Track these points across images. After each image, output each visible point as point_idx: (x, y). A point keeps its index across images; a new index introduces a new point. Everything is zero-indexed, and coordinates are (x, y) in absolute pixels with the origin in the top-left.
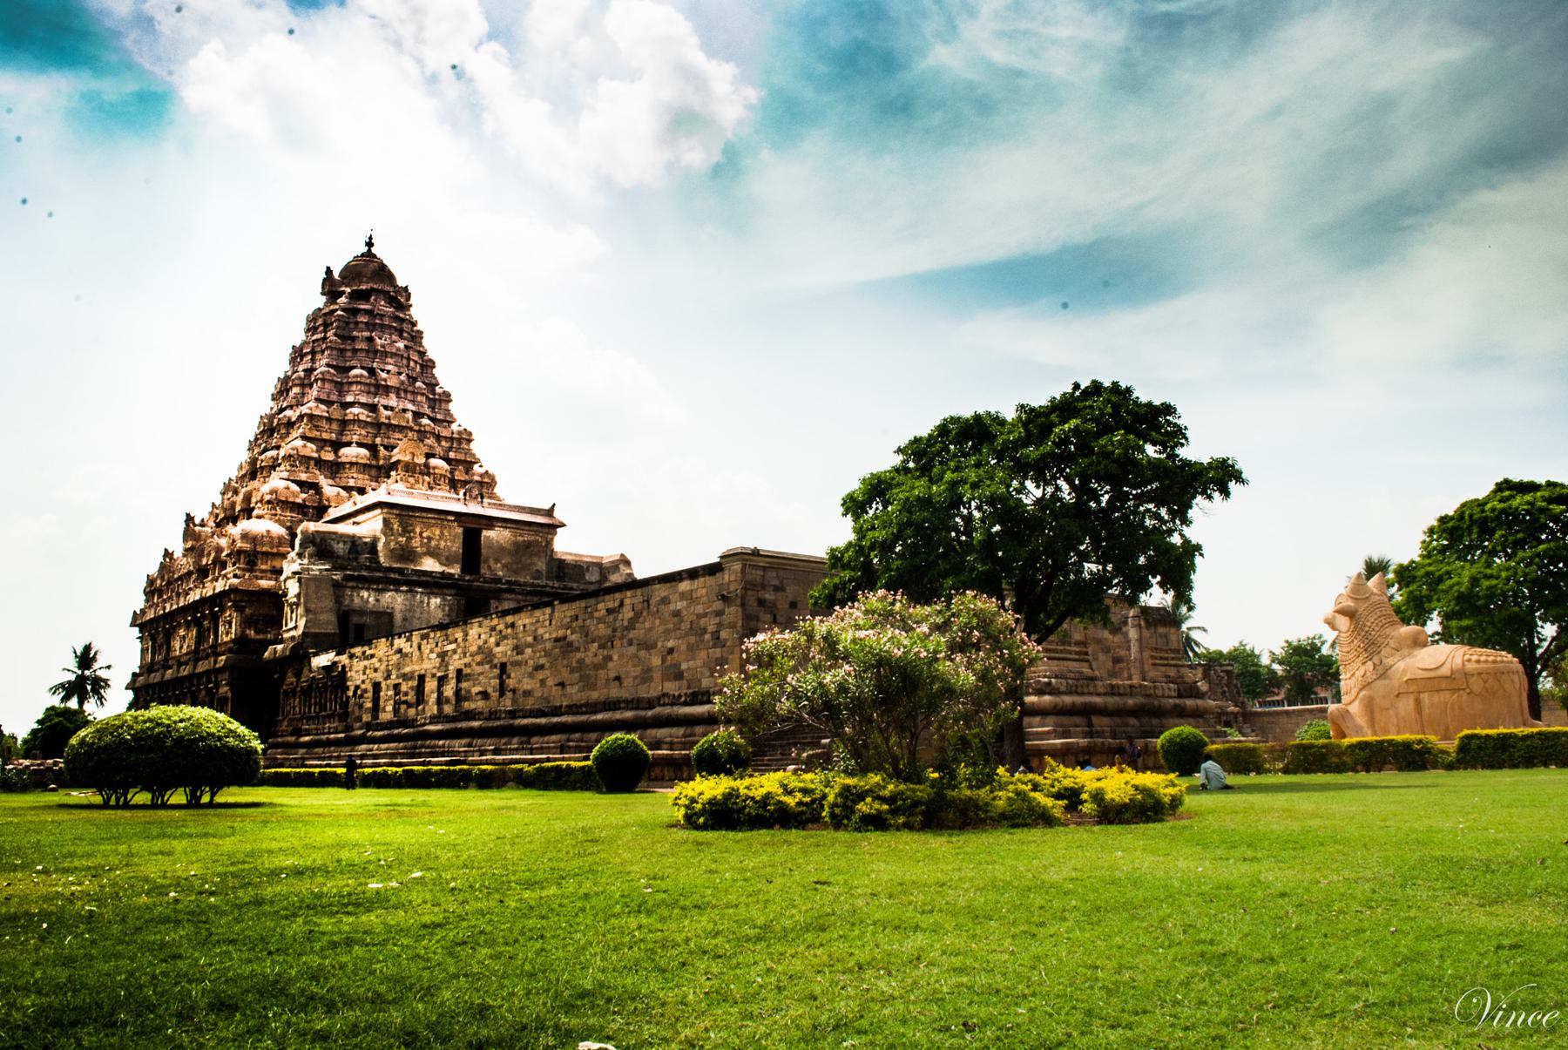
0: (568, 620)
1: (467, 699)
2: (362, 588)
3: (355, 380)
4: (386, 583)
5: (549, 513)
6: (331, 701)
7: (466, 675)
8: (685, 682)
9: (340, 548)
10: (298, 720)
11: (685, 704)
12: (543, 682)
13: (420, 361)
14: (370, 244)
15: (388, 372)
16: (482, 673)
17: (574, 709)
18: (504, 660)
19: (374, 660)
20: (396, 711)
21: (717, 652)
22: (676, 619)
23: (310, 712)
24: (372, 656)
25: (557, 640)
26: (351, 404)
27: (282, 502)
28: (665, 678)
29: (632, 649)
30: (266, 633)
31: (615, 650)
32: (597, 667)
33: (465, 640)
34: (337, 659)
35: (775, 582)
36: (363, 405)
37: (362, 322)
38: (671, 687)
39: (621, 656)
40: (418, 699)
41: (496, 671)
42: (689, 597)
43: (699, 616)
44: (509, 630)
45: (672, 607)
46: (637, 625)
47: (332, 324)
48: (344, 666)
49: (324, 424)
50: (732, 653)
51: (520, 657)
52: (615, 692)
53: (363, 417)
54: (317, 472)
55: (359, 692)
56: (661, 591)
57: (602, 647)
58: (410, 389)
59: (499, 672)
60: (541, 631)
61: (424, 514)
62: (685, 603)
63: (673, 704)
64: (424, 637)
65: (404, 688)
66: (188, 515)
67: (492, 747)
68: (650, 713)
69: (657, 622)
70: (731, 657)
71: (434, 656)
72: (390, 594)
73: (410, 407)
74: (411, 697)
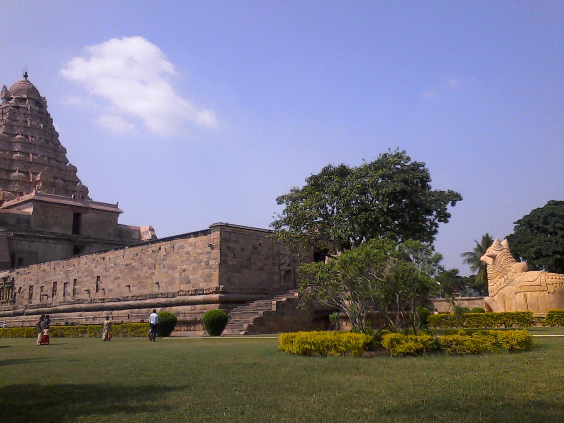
0: (133, 256)
1: (79, 294)
3: (19, 140)
5: (116, 206)
7: (79, 282)
8: (191, 284)
11: (191, 295)
12: (119, 285)
14: (26, 76)
16: (87, 281)
17: (135, 297)
19: (30, 275)
20: (41, 299)
21: (207, 271)
22: (187, 256)
24: (29, 273)
25: (127, 265)
26: (16, 152)
29: (165, 270)
31: (156, 270)
32: (147, 278)
33: (78, 265)
34: (9, 274)
38: (184, 287)
39: (159, 273)
42: (194, 245)
45: (185, 250)
46: (168, 258)
48: (13, 278)
50: (215, 271)
51: (107, 273)
52: (156, 290)
55: (21, 290)
56: (179, 242)
60: (118, 261)
62: (192, 248)
63: (185, 295)
65: (45, 288)
69: (178, 257)
70: (214, 273)
71: (62, 273)
73: (46, 154)
74: (50, 293)
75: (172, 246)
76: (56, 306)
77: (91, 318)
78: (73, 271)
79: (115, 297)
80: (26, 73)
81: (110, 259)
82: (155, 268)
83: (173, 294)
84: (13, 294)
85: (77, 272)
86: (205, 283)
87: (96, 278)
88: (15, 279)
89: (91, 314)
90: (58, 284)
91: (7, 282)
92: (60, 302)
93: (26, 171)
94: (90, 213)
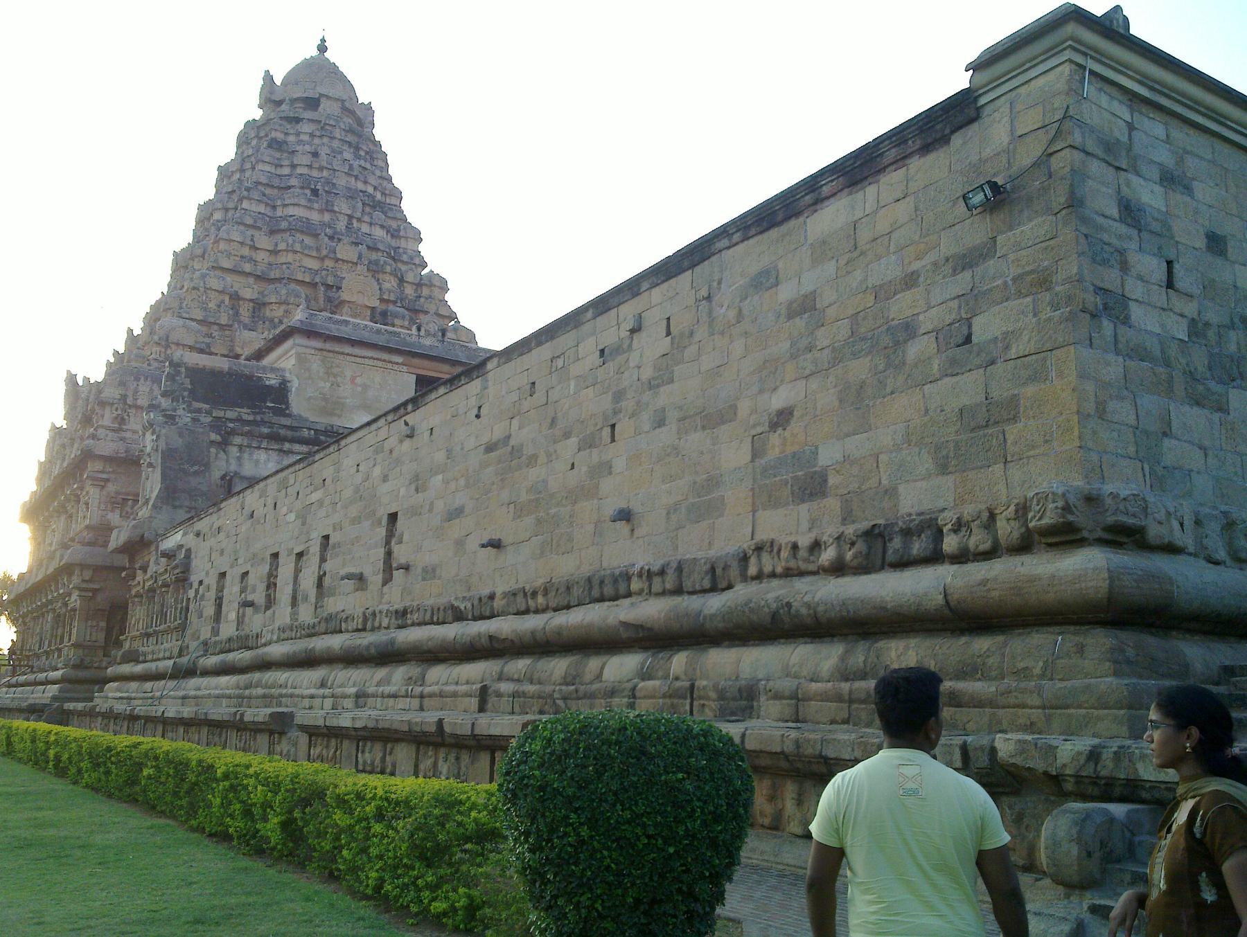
2: (259, 448)
8: (832, 504)
11: (839, 569)
12: (460, 543)
14: (322, 48)
20: (240, 622)
25: (490, 448)
27: (178, 344)
28: (763, 498)
29: (666, 436)
35: (1164, 156)
41: (382, 532)
43: (883, 293)
45: (786, 293)
48: (189, 551)
57: (588, 443)
58: (366, 218)
59: (384, 533)
62: (830, 268)
63: (788, 573)
64: (284, 486)
65: (251, 579)
67: (353, 690)
68: (715, 604)
70: (1030, 390)
74: (259, 597)
75: (704, 293)
79: (443, 601)
80: (323, 40)
82: (613, 440)
83: (713, 570)
86: (948, 481)
87: (385, 521)
88: (193, 556)
89: (350, 679)
90: (281, 560)
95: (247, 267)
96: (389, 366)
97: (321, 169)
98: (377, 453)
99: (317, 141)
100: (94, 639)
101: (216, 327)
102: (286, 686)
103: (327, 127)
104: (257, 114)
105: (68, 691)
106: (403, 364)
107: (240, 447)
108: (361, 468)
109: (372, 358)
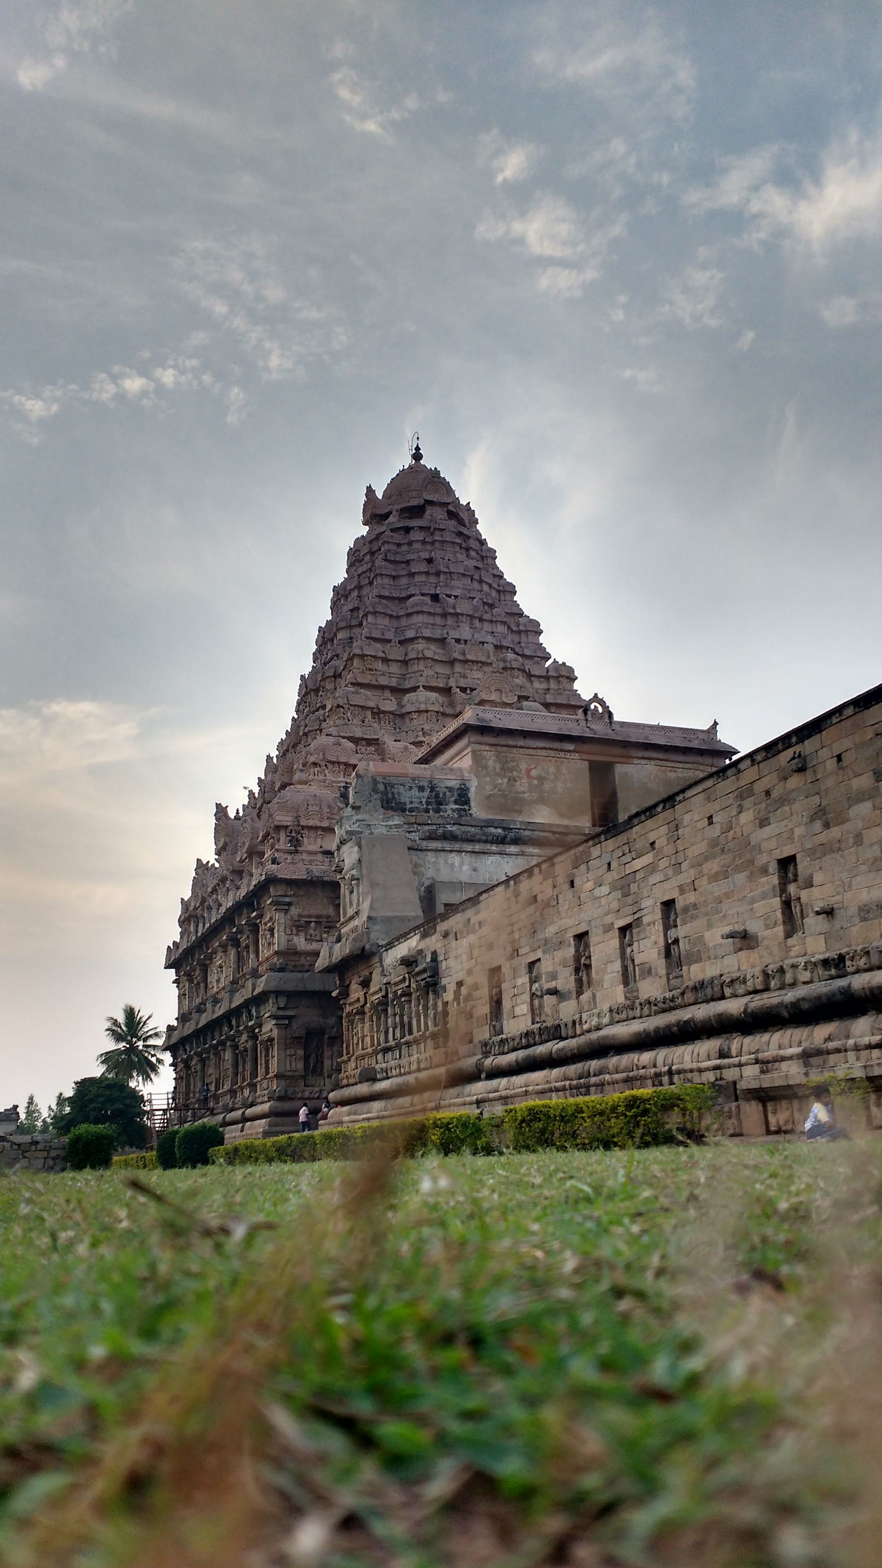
2: (451, 851)
3: (415, 609)
4: (486, 842)
6: (418, 1015)
7: (686, 910)
9: (410, 797)
10: (370, 1055)
13: (497, 587)
14: (417, 456)
15: (456, 597)
16: (727, 895)
18: (787, 852)
23: (387, 1041)
26: (412, 640)
27: (333, 763)
30: (321, 941)
36: (428, 639)
37: (417, 541)
40: (579, 982)
44: (795, 781)
47: (380, 549)
48: (434, 954)
49: (379, 665)
51: (835, 832)
53: (428, 654)
54: (375, 725)
55: (464, 990)
59: (775, 880)
61: (530, 743)
65: (546, 966)
66: (218, 806)
67: (799, 1050)
72: (492, 858)
74: (566, 981)
76: (598, 1028)
77: (791, 1058)
78: (651, 868)
81: (839, 758)
84: (440, 1008)
85: (670, 872)
87: (773, 867)
88: (441, 958)
90: (593, 939)
91: (417, 970)
92: (611, 1011)
93: (441, 685)
94: (636, 761)
95: (383, 681)
96: (562, 754)
97: (438, 574)
98: (742, 799)
99: (429, 547)
100: (294, 1068)
101: (364, 743)
102: (655, 1066)
103: (436, 533)
104: (364, 530)
105: (276, 1125)
106: (573, 751)
107: (436, 850)
108: (715, 820)
109: (544, 748)
